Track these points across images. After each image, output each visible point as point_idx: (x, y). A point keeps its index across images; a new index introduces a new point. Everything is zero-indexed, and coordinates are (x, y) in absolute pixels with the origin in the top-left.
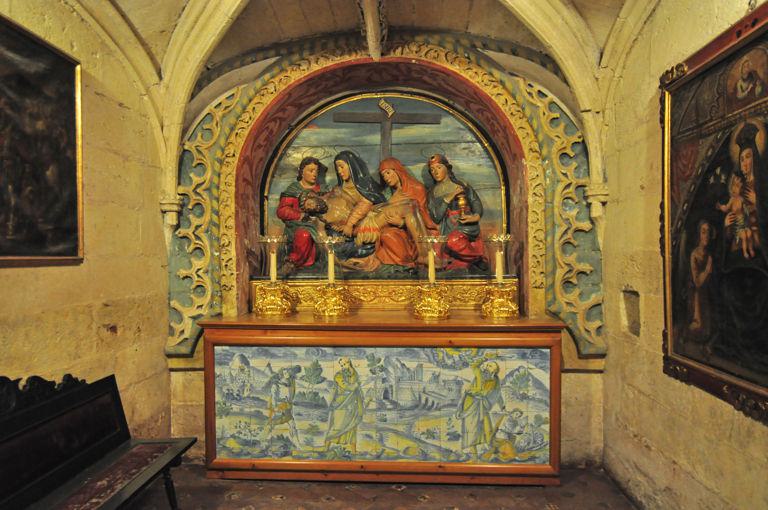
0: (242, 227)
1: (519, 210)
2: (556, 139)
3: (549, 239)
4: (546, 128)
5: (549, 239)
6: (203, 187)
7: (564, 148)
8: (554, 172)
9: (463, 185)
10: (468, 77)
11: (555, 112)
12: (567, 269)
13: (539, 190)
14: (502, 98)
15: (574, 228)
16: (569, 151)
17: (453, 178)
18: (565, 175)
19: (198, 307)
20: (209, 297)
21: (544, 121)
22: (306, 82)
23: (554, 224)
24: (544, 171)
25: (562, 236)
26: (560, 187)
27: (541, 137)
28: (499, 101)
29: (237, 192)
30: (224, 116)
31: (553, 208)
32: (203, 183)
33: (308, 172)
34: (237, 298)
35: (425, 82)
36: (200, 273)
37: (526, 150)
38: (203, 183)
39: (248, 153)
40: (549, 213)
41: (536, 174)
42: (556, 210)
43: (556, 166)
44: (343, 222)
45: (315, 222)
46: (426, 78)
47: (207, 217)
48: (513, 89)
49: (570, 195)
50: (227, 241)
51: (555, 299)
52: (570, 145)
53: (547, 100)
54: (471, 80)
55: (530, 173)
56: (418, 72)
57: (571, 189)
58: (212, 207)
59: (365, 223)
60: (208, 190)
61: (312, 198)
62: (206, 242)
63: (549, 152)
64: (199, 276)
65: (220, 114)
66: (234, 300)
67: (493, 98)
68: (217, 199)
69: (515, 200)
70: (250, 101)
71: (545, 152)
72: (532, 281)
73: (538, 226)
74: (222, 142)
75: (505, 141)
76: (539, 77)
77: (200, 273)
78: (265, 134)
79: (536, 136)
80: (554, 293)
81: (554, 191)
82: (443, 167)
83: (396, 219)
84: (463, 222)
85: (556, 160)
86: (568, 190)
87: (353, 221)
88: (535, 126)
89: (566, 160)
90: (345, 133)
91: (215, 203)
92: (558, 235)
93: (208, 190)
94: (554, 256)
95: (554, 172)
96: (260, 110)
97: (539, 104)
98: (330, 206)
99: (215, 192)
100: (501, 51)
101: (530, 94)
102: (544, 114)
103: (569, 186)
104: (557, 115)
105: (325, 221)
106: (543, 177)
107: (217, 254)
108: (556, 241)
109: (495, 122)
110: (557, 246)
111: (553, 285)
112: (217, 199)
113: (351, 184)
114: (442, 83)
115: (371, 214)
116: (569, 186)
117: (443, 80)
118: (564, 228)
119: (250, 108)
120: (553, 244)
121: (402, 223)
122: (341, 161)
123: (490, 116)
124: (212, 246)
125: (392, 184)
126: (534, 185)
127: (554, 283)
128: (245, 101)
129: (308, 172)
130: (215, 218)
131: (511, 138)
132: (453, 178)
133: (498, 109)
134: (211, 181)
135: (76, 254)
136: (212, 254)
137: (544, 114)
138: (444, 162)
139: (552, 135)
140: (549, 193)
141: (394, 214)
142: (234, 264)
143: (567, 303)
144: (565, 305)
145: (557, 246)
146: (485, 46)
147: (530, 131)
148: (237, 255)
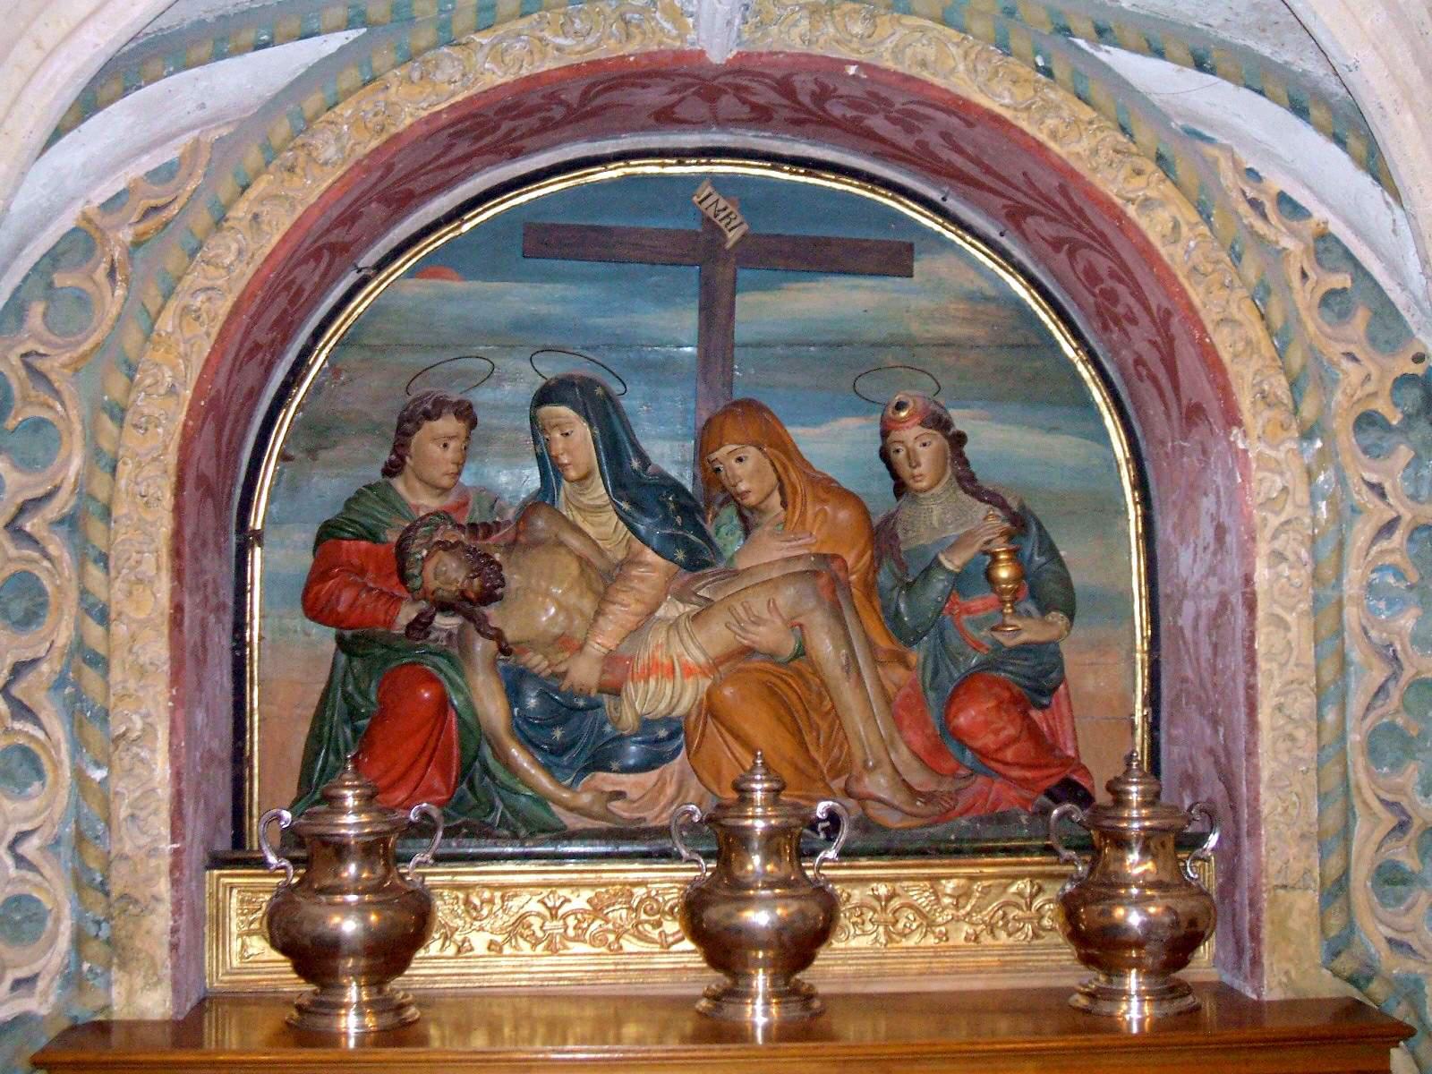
0: (189, 663)
1: (1210, 604)
2: (1346, 365)
3: (1331, 716)
4: (1312, 324)
5: (1331, 716)
6: (53, 510)
7: (1374, 395)
8: (1341, 480)
9: (1003, 505)
10: (1042, 137)
11: (1335, 270)
12: (1389, 820)
13: (1292, 544)
14: (1163, 216)
15: (1408, 674)
16: (1382, 406)
17: (967, 481)
18: (1378, 490)
19: (18, 984)
20: (63, 943)
21: (1304, 297)
22: (452, 125)
23: (1344, 663)
24: (1310, 475)
25: (1368, 709)
26: (1361, 533)
27: (1296, 358)
28: (1154, 226)
29: (177, 534)
30: (137, 244)
31: (1340, 605)
32: (49, 496)
33: (435, 450)
34: (174, 947)
35: (870, 135)
37: (1245, 401)
38: (49, 496)
39: (221, 381)
40: (1328, 624)
41: (1279, 483)
42: (1351, 614)
43: (1346, 459)
45: (459, 639)
46: (877, 123)
47: (61, 629)
48: (1202, 188)
49: (1389, 559)
50: (138, 723)
51: (1350, 926)
52: (1389, 384)
53: (1308, 228)
54: (1052, 145)
55: (1266, 484)
56: (853, 103)
57: (1399, 537)
58: (84, 592)
59: (656, 645)
60: (71, 523)
61: (445, 546)
62: (58, 728)
63: (1324, 409)
65: (127, 235)
66: (162, 953)
67: (1131, 211)
68: (103, 559)
69: (1186, 563)
70: (245, 188)
71: (1308, 410)
72: (1273, 867)
73: (1292, 672)
74: (132, 339)
75: (1152, 357)
76: (1281, 150)
77: (29, 848)
78: (282, 301)
79: (1281, 353)
80: (1348, 910)
81: (1341, 545)
82: (937, 440)
83: (770, 635)
84: (1009, 641)
85: (1346, 439)
86: (1384, 544)
88: (1277, 319)
89: (1372, 435)
90: (564, 300)
91: (95, 572)
92: (1356, 704)
93: (71, 523)
94: (1345, 776)
95: (1341, 480)
96: (279, 224)
97: (1287, 242)
98: (514, 579)
99: (96, 530)
100: (1160, 54)
101: (1255, 204)
102: (1304, 275)
103: (1389, 528)
104: (1342, 280)
105: (498, 636)
106: (1302, 495)
107: (98, 775)
108: (1350, 724)
109: (1121, 289)
110: (1355, 738)
111: (1342, 882)
112: (103, 559)
113: (598, 492)
114: (934, 141)
115: (671, 610)
116: (1389, 528)
117: (945, 136)
118: (1378, 675)
119: (241, 211)
120: (1342, 737)
121: (790, 646)
122: (564, 410)
123: (1103, 265)
124: (79, 743)
125: (752, 499)
126: (1274, 521)
127: (1345, 873)
128: (226, 189)
129: (435, 450)
130: (95, 631)
131: (1187, 357)
132: (967, 481)
133: (1147, 252)
134: (82, 490)
135: (198, 1044)
136: (80, 776)
137: (1304, 275)
138: (940, 423)
139: (1336, 349)
140: (1327, 551)
141: (766, 615)
142: (165, 815)
143: (1390, 941)
144: (1384, 945)
145: (1355, 738)
146: (1102, 33)
147: (1257, 331)
148: (177, 776)
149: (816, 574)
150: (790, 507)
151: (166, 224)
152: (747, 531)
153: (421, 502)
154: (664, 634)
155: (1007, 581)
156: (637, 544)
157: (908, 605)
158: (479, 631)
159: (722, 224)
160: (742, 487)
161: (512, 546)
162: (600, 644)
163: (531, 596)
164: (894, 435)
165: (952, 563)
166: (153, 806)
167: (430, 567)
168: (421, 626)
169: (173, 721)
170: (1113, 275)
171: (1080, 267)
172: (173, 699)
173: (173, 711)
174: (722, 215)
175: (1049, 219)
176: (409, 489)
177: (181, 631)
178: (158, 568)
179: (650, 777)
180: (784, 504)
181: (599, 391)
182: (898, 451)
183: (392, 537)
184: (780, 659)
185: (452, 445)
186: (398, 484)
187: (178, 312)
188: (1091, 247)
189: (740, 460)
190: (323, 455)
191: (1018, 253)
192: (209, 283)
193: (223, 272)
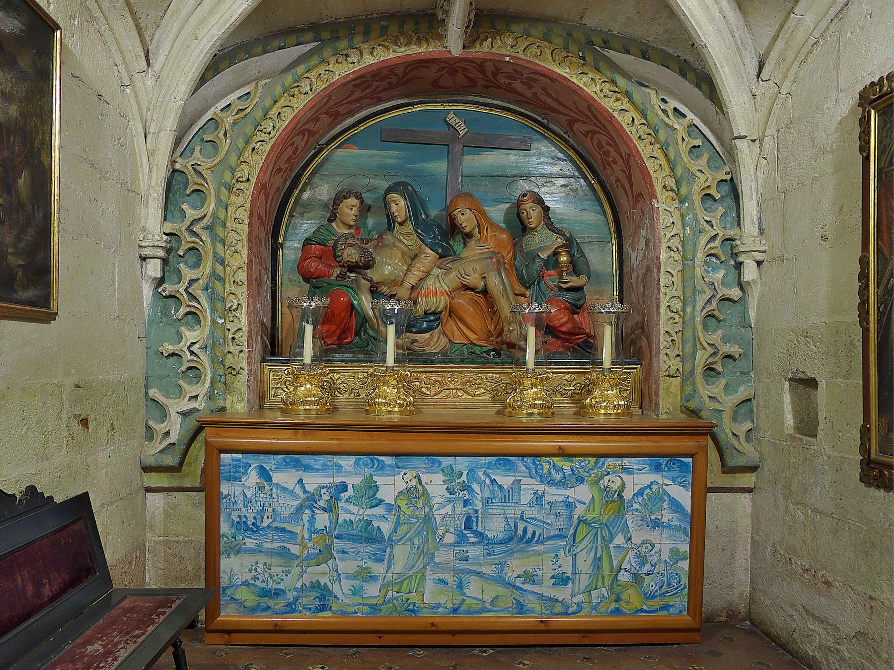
0: (255, 283)
2: (699, 174)
4: (686, 158)
5: (689, 310)
6: (203, 223)
7: (709, 187)
9: (564, 235)
10: (581, 85)
12: (711, 350)
13: (675, 243)
16: (713, 192)
17: (550, 226)
19: (191, 398)
20: (208, 384)
21: (683, 148)
22: (354, 80)
24: (683, 216)
25: (704, 308)
26: (704, 239)
27: (679, 171)
28: (623, 120)
29: (250, 233)
30: (235, 123)
32: (202, 218)
33: (347, 210)
34: (249, 387)
35: (515, 92)
36: (194, 348)
37: (658, 188)
38: (202, 218)
39: (266, 179)
42: (698, 271)
44: (397, 282)
46: (517, 85)
47: (207, 268)
49: (713, 251)
53: (685, 122)
54: (585, 88)
55: (664, 220)
56: (509, 77)
57: (717, 242)
58: (215, 253)
59: (430, 284)
60: (209, 228)
62: (206, 304)
64: (192, 353)
65: (230, 119)
66: (244, 389)
67: (615, 114)
68: (223, 242)
69: (634, 258)
70: (275, 102)
71: (683, 191)
72: (664, 367)
74: (233, 160)
77: (195, 348)
78: (289, 151)
79: (672, 169)
80: (694, 383)
81: (695, 244)
82: (539, 209)
83: (474, 280)
84: (564, 286)
86: (712, 245)
87: (412, 280)
88: (672, 155)
89: (709, 203)
90: (397, 158)
91: (219, 246)
93: (209, 228)
95: (696, 219)
96: (289, 116)
97: (676, 126)
98: (378, 259)
99: (219, 230)
100: (628, 52)
101: (664, 111)
102: (683, 139)
103: (713, 238)
104: (698, 142)
105: (370, 280)
106: (680, 226)
107: (221, 321)
108: (697, 313)
110: (698, 319)
111: (692, 372)
112: (223, 242)
113: (409, 227)
114: (540, 92)
115: (436, 271)
116: (713, 238)
117: (543, 88)
119: (273, 113)
121: (481, 285)
123: (604, 139)
124: (213, 310)
125: (467, 230)
126: (669, 235)
128: (268, 102)
129: (347, 210)
130: (219, 268)
131: (636, 172)
132: (550, 226)
133: (620, 131)
134: (215, 216)
136: (214, 322)
137: (683, 139)
139: (694, 169)
142: (245, 338)
143: (710, 397)
144: (707, 400)
145: (698, 319)
146: (606, 44)
147: (663, 162)
148: (250, 323)
149: (492, 258)
150: (482, 234)
151: (246, 116)
152: (465, 245)
153: (342, 231)
154: (433, 280)
155: (564, 262)
156: (423, 246)
157: (526, 271)
158: (363, 278)
159: (458, 129)
160: (463, 225)
161: (376, 247)
163: (384, 265)
164: (522, 207)
165: (544, 255)
166: (241, 334)
167: (345, 253)
168: (342, 276)
169: (248, 303)
170: (608, 144)
171: (595, 143)
172: (248, 295)
173: (248, 299)
174: (458, 125)
175: (584, 123)
176: (338, 227)
177: (252, 270)
178: (243, 246)
179: (427, 336)
180: (480, 233)
181: (410, 188)
182: (523, 213)
183: (331, 243)
184: (478, 290)
185: (354, 209)
186: (334, 224)
187: (251, 149)
188: (600, 133)
189: (463, 214)
190: (305, 215)
192: (262, 139)
193: (267, 135)
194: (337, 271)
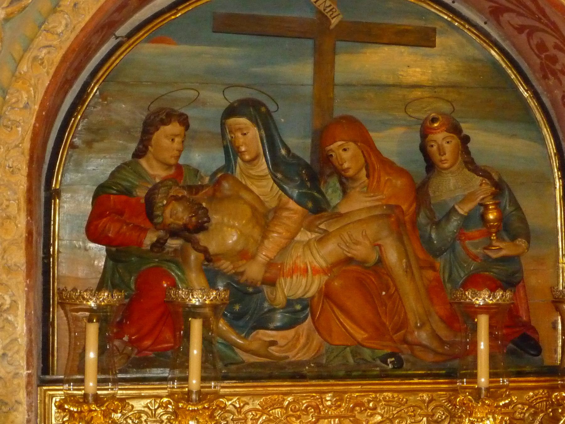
33: (166, 142)
45: (181, 253)
50: (8, 301)
61: (177, 199)
82: (455, 141)
84: (494, 255)
98: (215, 218)
105: (205, 251)
113: (263, 167)
115: (304, 236)
121: (373, 257)
122: (243, 121)
125: (351, 173)
129: (166, 142)
138: (455, 129)
141: (360, 239)
142: (23, 354)
149: (389, 216)
150: (371, 178)
151: (25, 8)
152: (345, 192)
153: (156, 173)
154: (301, 250)
155: (494, 221)
156: (285, 198)
157: (437, 234)
158: (194, 248)
159: (328, 15)
160: (346, 165)
161: (212, 198)
162: (262, 257)
163: (225, 229)
164: (431, 137)
165: (463, 210)
166: (16, 348)
167: (168, 212)
168: (159, 245)
169: (28, 299)
170: (556, 47)
171: (534, 41)
172: (27, 286)
173: (28, 293)
174: (328, 9)
175: (519, 14)
176: (151, 167)
177: (32, 247)
178: (19, 210)
179: (290, 333)
180: (368, 176)
181: (263, 109)
182: (432, 146)
183: (141, 193)
184: (367, 265)
185: (177, 140)
186: (143, 162)
187: (31, 59)
188: (543, 31)
189: (345, 150)
190: (96, 145)
191: (495, 35)
192: (49, 43)
193: (56, 36)
194: (150, 238)
